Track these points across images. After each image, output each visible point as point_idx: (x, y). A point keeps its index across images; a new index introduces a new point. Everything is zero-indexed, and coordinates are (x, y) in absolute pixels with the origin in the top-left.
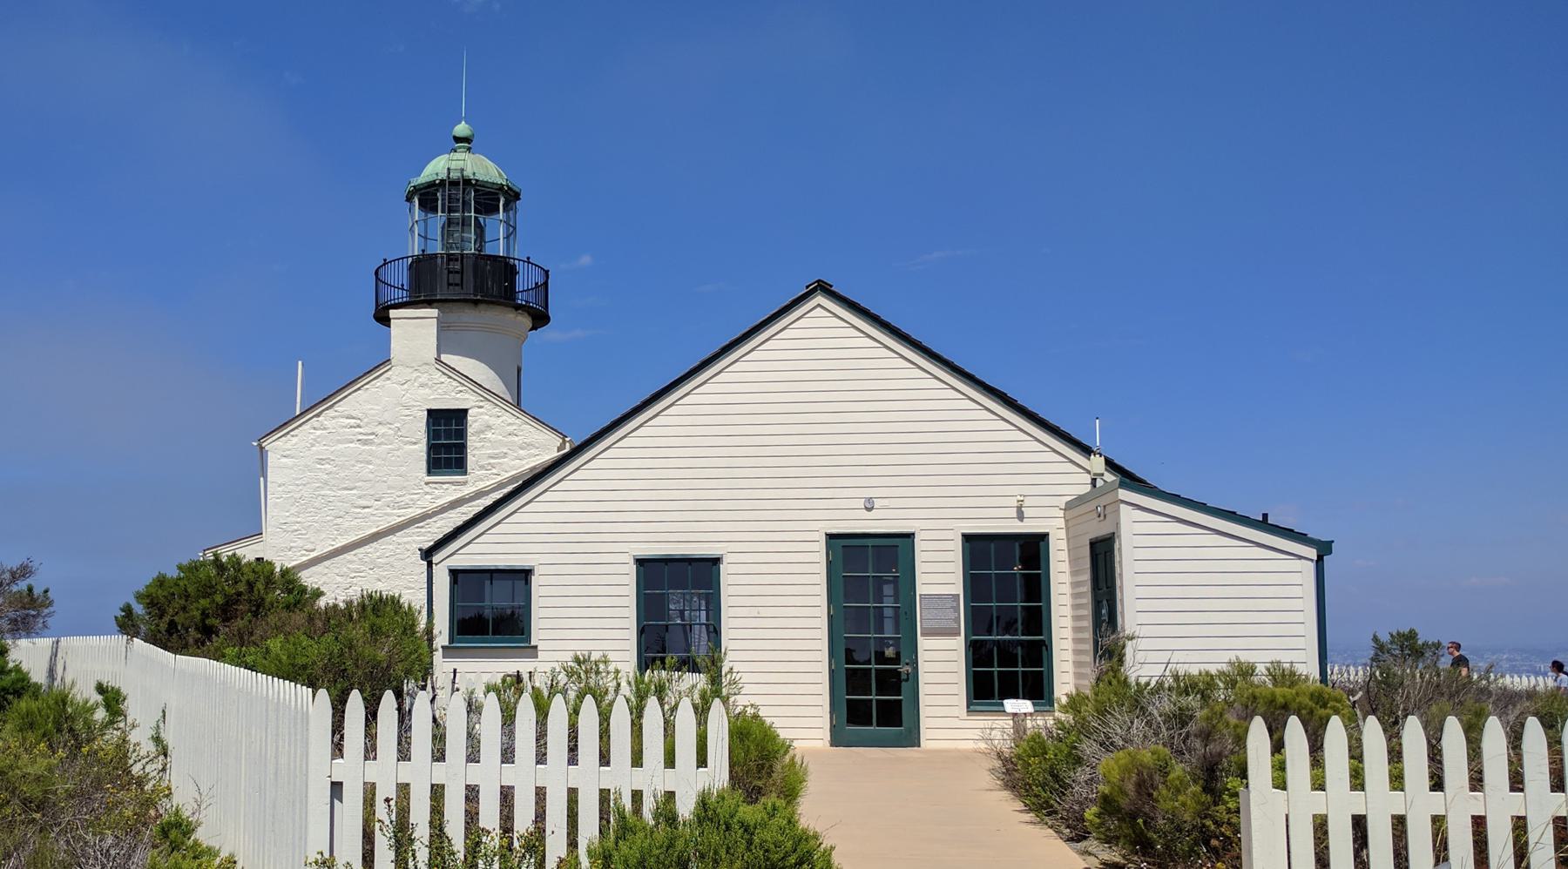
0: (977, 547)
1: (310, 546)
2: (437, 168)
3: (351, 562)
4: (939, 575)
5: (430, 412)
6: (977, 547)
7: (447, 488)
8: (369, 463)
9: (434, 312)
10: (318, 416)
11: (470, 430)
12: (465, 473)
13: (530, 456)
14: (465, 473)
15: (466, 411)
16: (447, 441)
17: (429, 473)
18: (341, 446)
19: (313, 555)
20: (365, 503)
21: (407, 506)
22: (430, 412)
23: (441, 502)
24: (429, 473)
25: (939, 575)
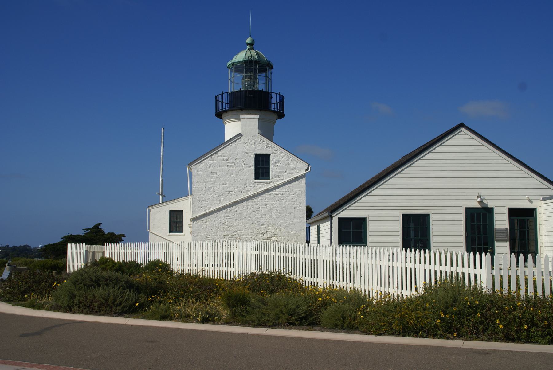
0: (514, 213)
1: (209, 206)
2: (241, 57)
3: (225, 213)
4: (501, 221)
5: (256, 155)
6: (514, 213)
7: (263, 185)
9: (257, 116)
10: (212, 155)
11: (272, 162)
15: (269, 155)
17: (256, 179)
19: (211, 210)
20: (232, 190)
21: (248, 191)
22: (256, 155)
23: (259, 190)
24: (256, 179)
25: (501, 221)
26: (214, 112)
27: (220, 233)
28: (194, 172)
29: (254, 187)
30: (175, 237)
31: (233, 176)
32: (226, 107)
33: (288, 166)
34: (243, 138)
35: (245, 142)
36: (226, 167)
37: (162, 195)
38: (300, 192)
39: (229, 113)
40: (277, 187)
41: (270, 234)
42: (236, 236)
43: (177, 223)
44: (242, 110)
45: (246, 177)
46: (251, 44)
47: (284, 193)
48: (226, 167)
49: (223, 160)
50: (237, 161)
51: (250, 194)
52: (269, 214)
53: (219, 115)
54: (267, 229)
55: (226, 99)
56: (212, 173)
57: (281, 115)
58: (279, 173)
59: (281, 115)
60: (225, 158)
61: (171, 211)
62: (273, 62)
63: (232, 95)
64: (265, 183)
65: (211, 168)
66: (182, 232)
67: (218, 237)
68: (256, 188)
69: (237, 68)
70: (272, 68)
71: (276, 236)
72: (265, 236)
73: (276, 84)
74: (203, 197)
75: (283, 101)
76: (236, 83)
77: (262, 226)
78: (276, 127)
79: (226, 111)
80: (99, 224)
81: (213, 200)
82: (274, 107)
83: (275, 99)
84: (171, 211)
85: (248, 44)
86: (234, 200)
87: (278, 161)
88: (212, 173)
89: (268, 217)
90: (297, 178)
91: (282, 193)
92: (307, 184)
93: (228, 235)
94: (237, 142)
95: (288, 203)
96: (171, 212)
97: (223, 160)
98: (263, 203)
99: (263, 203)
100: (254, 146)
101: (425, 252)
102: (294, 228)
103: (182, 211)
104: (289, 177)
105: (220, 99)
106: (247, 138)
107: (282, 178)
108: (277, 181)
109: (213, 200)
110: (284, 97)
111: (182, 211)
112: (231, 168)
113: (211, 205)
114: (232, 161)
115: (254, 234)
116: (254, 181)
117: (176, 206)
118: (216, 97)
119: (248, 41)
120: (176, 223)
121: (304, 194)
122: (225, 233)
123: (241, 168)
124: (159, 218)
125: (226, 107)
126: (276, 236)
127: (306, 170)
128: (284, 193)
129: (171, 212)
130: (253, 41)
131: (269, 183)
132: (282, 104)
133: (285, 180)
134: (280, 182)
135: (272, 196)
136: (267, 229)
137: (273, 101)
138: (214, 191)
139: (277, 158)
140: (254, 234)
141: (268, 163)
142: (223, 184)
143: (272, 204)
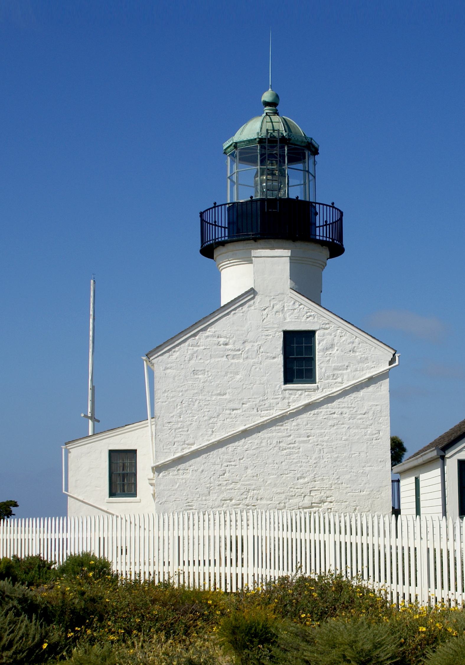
1: (191, 441)
3: (224, 453)
7: (300, 394)
8: (237, 373)
9: (288, 253)
10: (195, 335)
12: (314, 382)
13: (368, 368)
14: (314, 382)
16: (298, 356)
18: (213, 360)
19: (194, 448)
20: (236, 406)
23: (294, 406)
26: (199, 248)
27: (213, 496)
28: (158, 371)
29: (284, 399)
30: (122, 505)
31: (238, 377)
32: (222, 234)
33: (352, 354)
34: (258, 298)
35: (263, 306)
36: (224, 359)
37: (93, 418)
38: (379, 408)
39: (230, 246)
40: (329, 399)
41: (316, 496)
42: (247, 502)
43: (124, 476)
44: (255, 240)
45: (265, 378)
46: (273, 104)
47: (345, 410)
48: (224, 359)
49: (218, 344)
50: (248, 346)
51: (276, 413)
52: (316, 455)
53: (208, 251)
54: (310, 485)
55: (223, 219)
56: (195, 372)
57: (336, 249)
58: (335, 369)
59: (336, 249)
60: (222, 340)
61: (111, 452)
62: (318, 141)
64: (305, 390)
65: (192, 362)
67: (210, 503)
68: (286, 401)
69: (244, 153)
70: (315, 152)
71: (329, 499)
72: (307, 501)
73: (324, 185)
74: (178, 422)
75: (341, 219)
76: (244, 185)
77: (301, 481)
78: (326, 274)
79: (223, 244)
81: (198, 428)
82: (321, 233)
83: (323, 217)
84: (111, 452)
85: (267, 104)
86: (242, 428)
87: (332, 346)
88: (195, 372)
89: (312, 461)
90: (372, 381)
91: (340, 411)
92: (392, 392)
93: (231, 500)
94: (245, 307)
95: (352, 431)
96: (112, 453)
97: (218, 344)
98: (302, 432)
99: (302, 432)
100: (281, 315)
103: (135, 451)
104: (354, 378)
105: (209, 218)
106: (268, 299)
107: (339, 380)
108: (329, 386)
110: (342, 213)
111: (135, 451)
112: (235, 361)
115: (283, 496)
116: (284, 387)
117: (121, 441)
118: (201, 214)
119: (267, 96)
120: (122, 475)
121: (387, 412)
122: (225, 495)
123: (256, 360)
124: (87, 466)
125: (222, 234)
126: (329, 499)
127: (391, 363)
128: (345, 410)
129: (112, 453)
130: (277, 96)
131: (314, 390)
132: (338, 226)
133: (347, 384)
134: (336, 389)
135: (320, 418)
136: (310, 485)
137: (319, 221)
139: (330, 338)
140: (283, 496)
141: (311, 349)
142: (220, 394)
143: (321, 435)
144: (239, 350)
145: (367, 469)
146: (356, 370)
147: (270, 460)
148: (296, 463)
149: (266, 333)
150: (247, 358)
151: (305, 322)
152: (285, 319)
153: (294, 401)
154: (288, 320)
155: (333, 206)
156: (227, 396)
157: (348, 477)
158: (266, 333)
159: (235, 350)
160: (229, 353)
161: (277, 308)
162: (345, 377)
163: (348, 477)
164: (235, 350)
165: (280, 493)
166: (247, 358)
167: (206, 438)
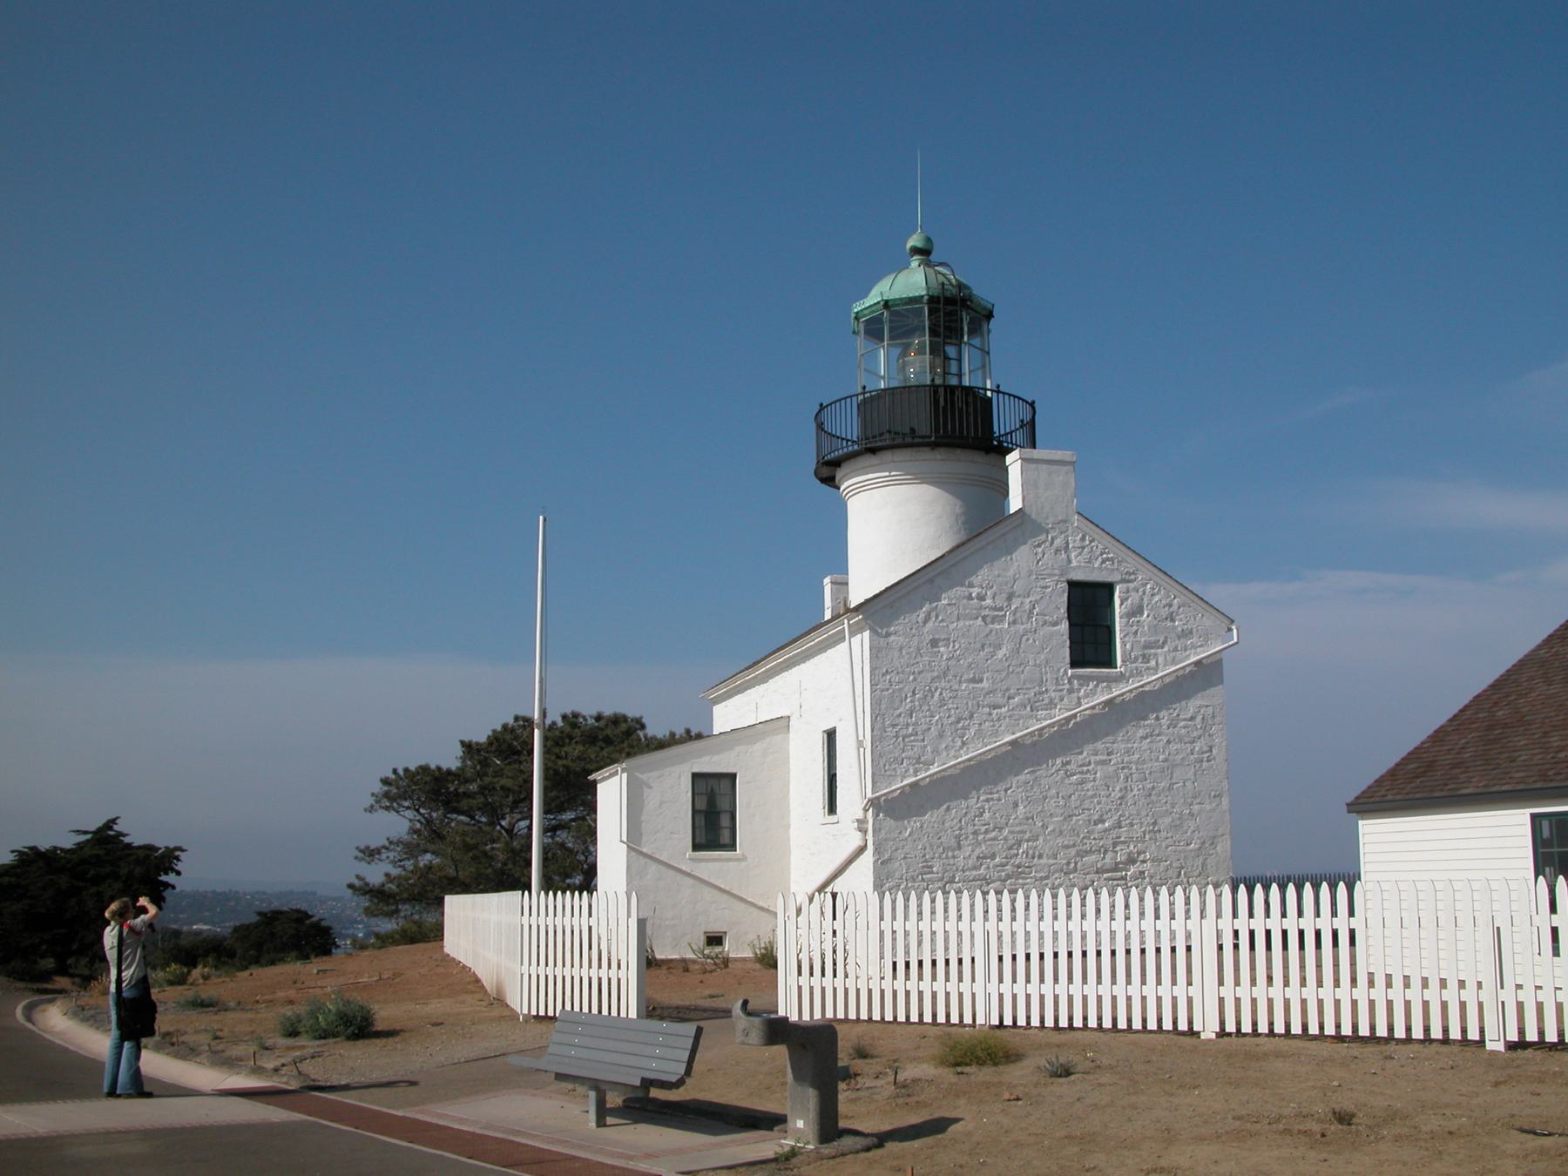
1: (929, 756)
8: (999, 647)
13: (1194, 647)
17: (1074, 664)
18: (961, 624)
20: (1000, 701)
22: (1072, 585)
24: (1074, 664)
29: (1070, 691)
30: (712, 865)
46: (924, 252)
49: (970, 597)
54: (1114, 834)
56: (934, 643)
58: (1147, 646)
61: (695, 776)
63: (870, 404)
64: (1100, 680)
65: (930, 624)
66: (732, 846)
67: (960, 862)
71: (1141, 857)
76: (886, 367)
80: (114, 821)
81: (941, 735)
84: (695, 776)
85: (916, 251)
88: (934, 643)
89: (1116, 794)
93: (993, 857)
95: (1174, 747)
101: (1112, 894)
102: (1197, 829)
104: (1174, 662)
107: (1153, 663)
109: (941, 735)
113: (936, 751)
114: (999, 603)
115: (1073, 852)
118: (822, 407)
119: (915, 241)
126: (1141, 857)
130: (929, 240)
136: (1114, 834)
138: (942, 702)
140: (1073, 852)
142: (973, 680)
144: (1001, 609)
145: (1196, 808)
146: (1176, 649)
147: (1053, 791)
148: (1094, 796)
149: (1041, 583)
150: (1014, 622)
151: (1100, 568)
152: (1070, 561)
153: (1086, 696)
154: (1074, 564)
155: (1032, 405)
156: (985, 684)
157: (1168, 820)
158: (1041, 583)
159: (995, 609)
160: (986, 612)
161: (1058, 542)
162: (1161, 660)
163: (1168, 820)
164: (995, 609)
165: (1067, 847)
166: (1014, 622)
167: (952, 753)
